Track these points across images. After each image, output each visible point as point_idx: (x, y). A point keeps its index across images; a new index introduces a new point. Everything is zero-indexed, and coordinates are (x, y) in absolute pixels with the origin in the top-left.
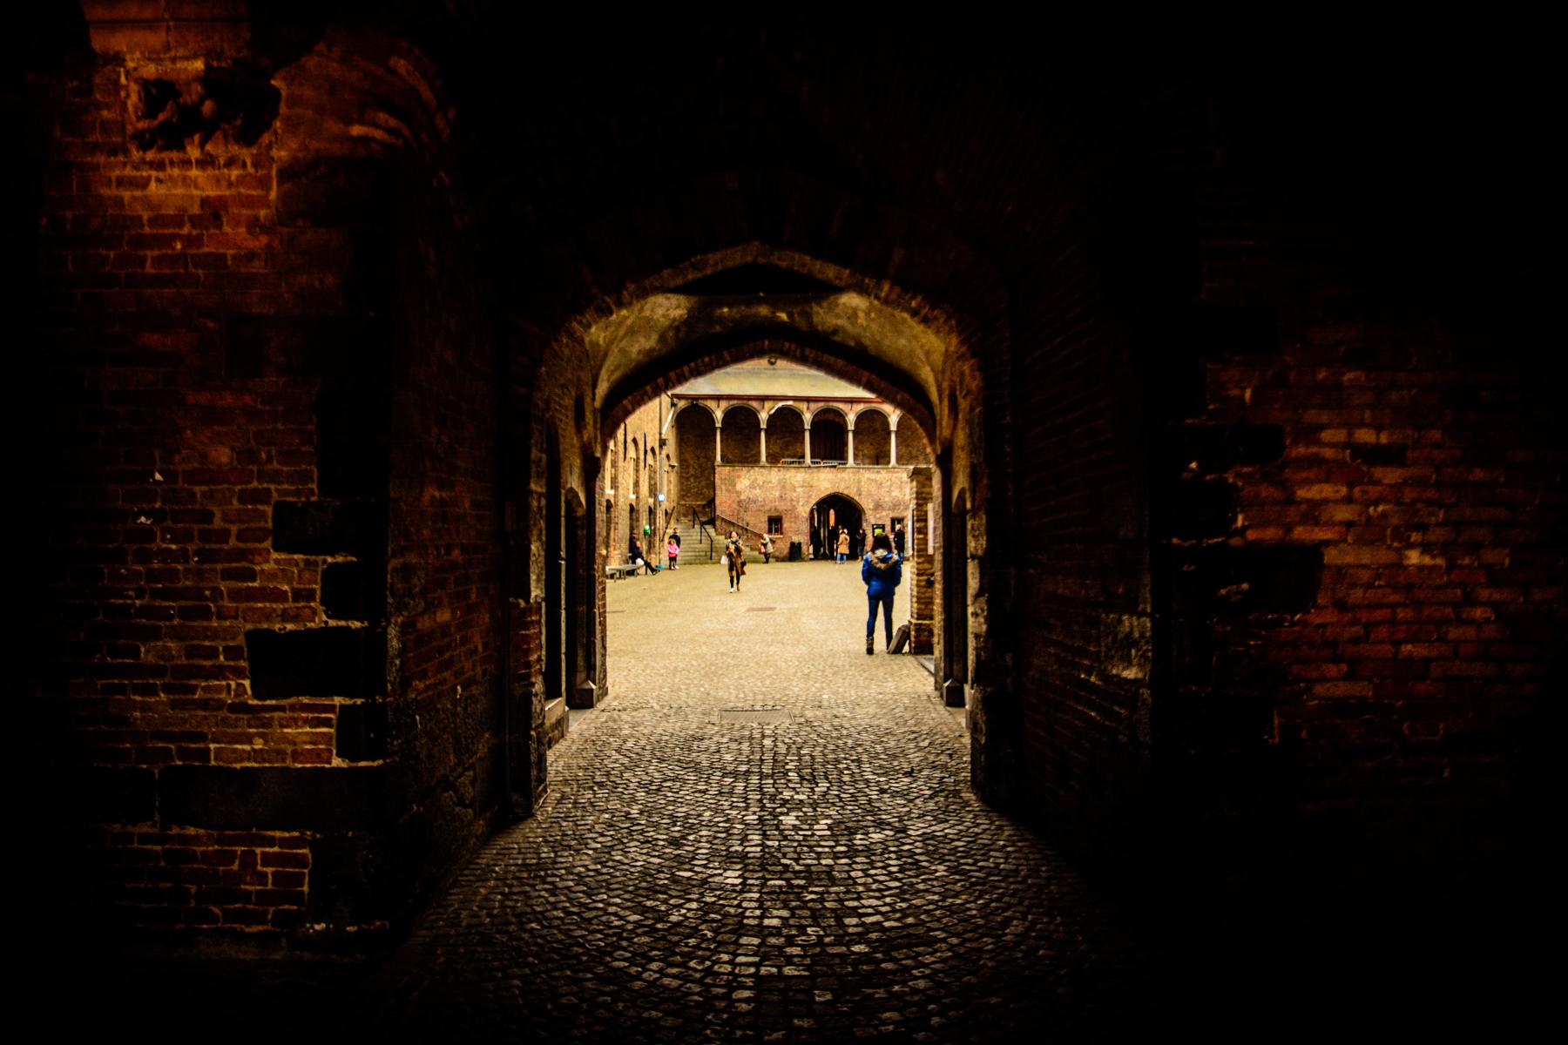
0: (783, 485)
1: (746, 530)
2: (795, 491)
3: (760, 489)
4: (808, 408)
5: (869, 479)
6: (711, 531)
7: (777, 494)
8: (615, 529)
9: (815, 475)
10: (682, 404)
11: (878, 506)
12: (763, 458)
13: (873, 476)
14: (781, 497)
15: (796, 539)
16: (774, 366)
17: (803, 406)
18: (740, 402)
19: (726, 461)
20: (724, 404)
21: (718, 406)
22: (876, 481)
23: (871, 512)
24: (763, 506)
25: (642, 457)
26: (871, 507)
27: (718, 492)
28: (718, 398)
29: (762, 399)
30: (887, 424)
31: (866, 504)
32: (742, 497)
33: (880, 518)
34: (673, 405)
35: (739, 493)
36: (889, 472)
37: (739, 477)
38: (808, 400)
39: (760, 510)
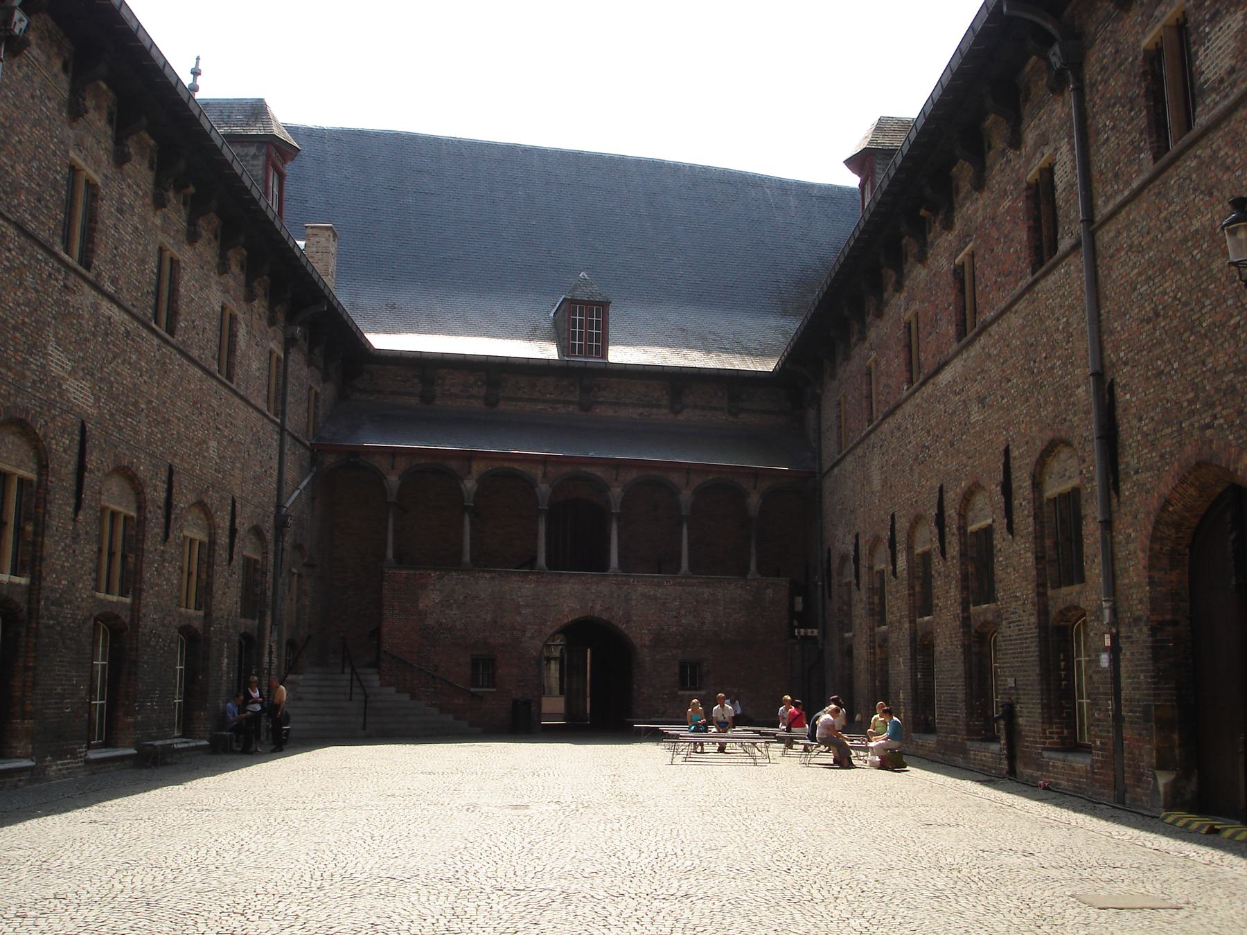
2: (519, 613)
4: (544, 475)
5: (644, 595)
6: (373, 679)
7: (489, 617)
10: (330, 460)
12: (467, 558)
14: (496, 622)
20: (402, 464)
21: (393, 468)
23: (646, 650)
25: (223, 539)
29: (470, 457)
31: (639, 635)
34: (314, 461)
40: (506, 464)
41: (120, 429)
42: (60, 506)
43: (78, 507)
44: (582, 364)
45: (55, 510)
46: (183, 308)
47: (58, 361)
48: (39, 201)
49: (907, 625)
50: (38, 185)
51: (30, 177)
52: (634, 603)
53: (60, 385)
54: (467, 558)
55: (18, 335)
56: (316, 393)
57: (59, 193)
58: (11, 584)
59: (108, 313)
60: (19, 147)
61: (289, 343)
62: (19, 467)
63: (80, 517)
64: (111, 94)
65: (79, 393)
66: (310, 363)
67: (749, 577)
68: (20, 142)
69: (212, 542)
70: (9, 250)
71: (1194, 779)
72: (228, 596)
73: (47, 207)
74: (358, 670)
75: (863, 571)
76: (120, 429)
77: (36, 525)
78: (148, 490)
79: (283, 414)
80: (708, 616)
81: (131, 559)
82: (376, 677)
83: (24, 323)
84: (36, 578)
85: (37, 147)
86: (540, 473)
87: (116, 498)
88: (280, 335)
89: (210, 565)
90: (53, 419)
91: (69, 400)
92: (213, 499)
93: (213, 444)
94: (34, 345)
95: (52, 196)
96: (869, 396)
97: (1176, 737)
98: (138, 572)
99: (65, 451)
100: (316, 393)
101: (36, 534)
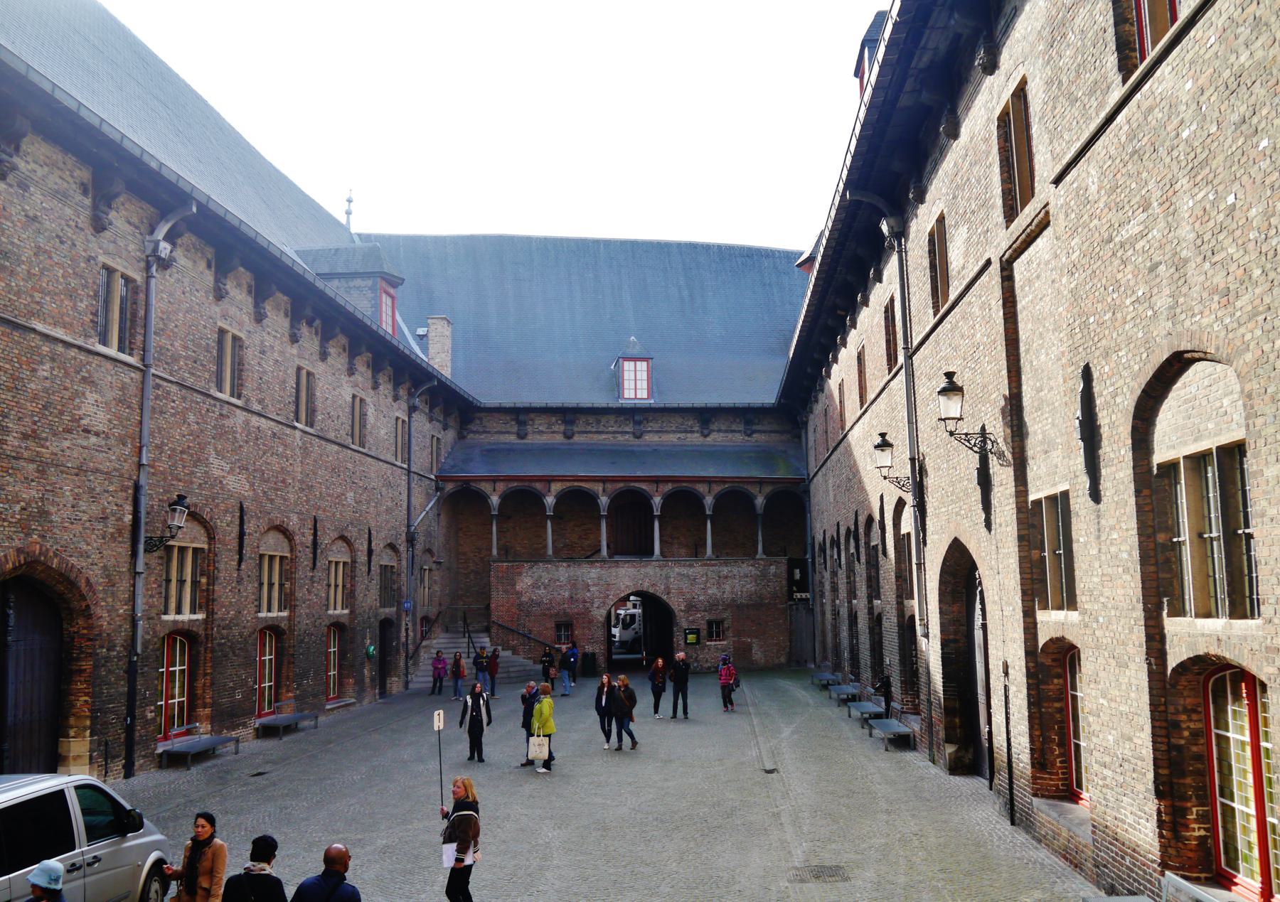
0: (573, 584)
1: (529, 638)
2: (589, 591)
3: (545, 588)
4: (604, 490)
5: (679, 574)
7: (567, 594)
8: (289, 663)
9: (613, 570)
10: (450, 487)
11: (691, 607)
13: (684, 571)
14: (572, 597)
15: (589, 649)
16: (572, 441)
17: (598, 488)
18: (520, 484)
19: (506, 552)
20: (501, 487)
21: (494, 490)
22: (688, 576)
23: (682, 614)
24: (549, 609)
25: (362, 558)
26: (683, 608)
27: (494, 594)
28: (494, 480)
29: (548, 480)
30: (702, 507)
32: (524, 599)
33: (693, 621)
34: (437, 489)
35: (519, 594)
36: (705, 565)
37: (520, 574)
38: (604, 480)
39: (545, 615)
40: (576, 484)
41: (272, 501)
42: (226, 563)
43: (240, 561)
44: (633, 406)
45: (222, 566)
46: (319, 404)
47: (217, 466)
48: (195, 362)
49: (846, 604)
50: (194, 352)
51: (186, 348)
52: (672, 580)
53: (221, 482)
54: (550, 552)
55: (184, 456)
56: (438, 439)
57: (211, 353)
58: (191, 621)
59: (257, 424)
60: (176, 330)
61: (412, 409)
62: (192, 542)
63: (243, 567)
64: (248, 273)
65: (237, 484)
66: (431, 420)
67: (758, 557)
68: (176, 326)
69: (354, 561)
70: (174, 401)
71: (971, 750)
72: (369, 595)
73: (202, 365)
74: (474, 640)
75: (828, 558)
76: (272, 501)
77: (208, 578)
78: (297, 538)
79: (409, 459)
80: (728, 588)
81: (287, 585)
82: (487, 640)
83: (189, 447)
84: (210, 613)
85: (190, 326)
86: (601, 488)
87: (273, 545)
88: (405, 406)
89: (353, 578)
90: (217, 506)
91: (229, 490)
92: (352, 533)
93: (350, 495)
94: (199, 460)
95: (205, 356)
96: (826, 432)
97: (957, 720)
98: (292, 593)
99: (228, 526)
100: (438, 439)
101: (208, 584)
